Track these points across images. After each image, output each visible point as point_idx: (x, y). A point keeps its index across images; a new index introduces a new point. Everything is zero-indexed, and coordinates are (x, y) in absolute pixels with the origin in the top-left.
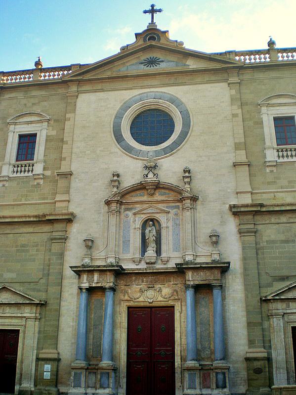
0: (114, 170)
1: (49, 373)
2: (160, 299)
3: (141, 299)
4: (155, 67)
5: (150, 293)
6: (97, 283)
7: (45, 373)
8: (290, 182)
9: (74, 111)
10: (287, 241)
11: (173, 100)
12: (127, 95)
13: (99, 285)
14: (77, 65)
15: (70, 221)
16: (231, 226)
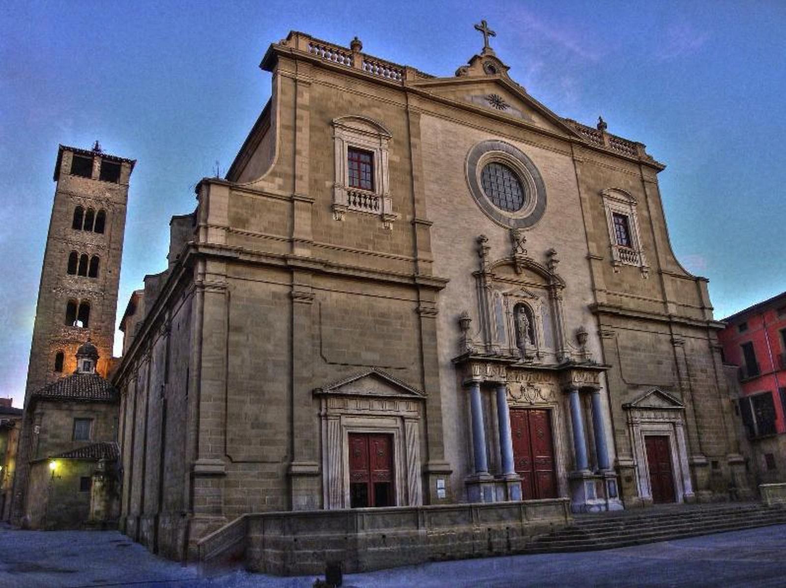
0: (484, 234)
1: (443, 491)
2: (540, 400)
3: (523, 399)
4: (501, 111)
5: (532, 393)
6: (491, 376)
7: (439, 491)
8: (631, 287)
9: (418, 135)
10: (635, 349)
11: (525, 159)
12: (486, 137)
13: (493, 379)
14: (414, 69)
15: (437, 289)
16: (591, 327)
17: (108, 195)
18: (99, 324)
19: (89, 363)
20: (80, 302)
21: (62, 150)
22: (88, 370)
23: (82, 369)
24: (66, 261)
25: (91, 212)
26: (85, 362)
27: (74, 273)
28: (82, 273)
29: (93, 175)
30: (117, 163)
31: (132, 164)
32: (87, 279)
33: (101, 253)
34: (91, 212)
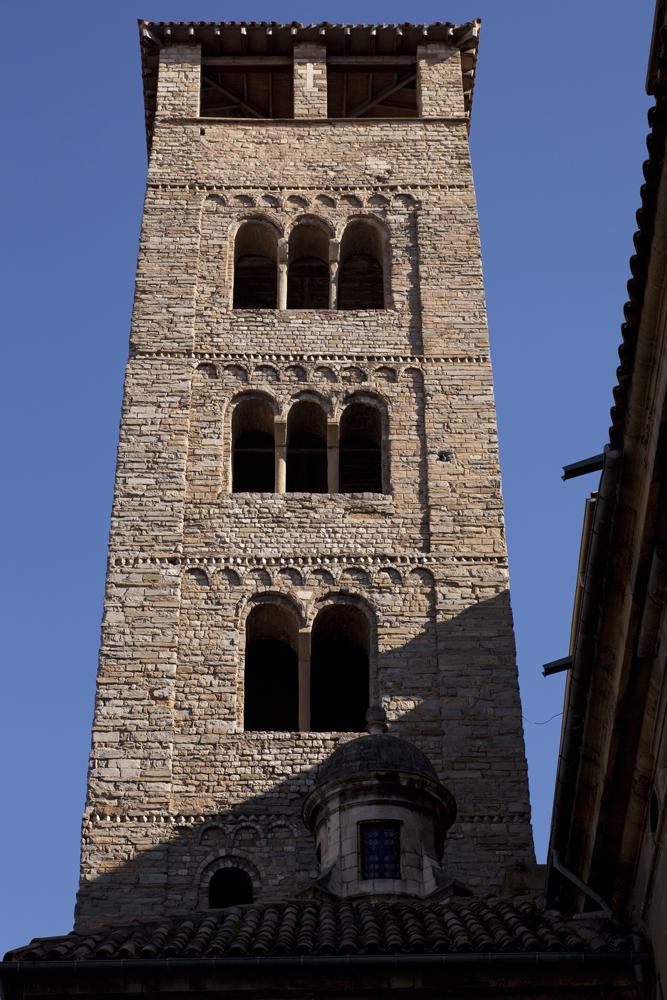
17: (378, 165)
18: (433, 704)
19: (396, 825)
20: (311, 612)
21: (158, 43)
22: (396, 874)
23: (351, 870)
24: (220, 443)
25: (311, 232)
26: (364, 827)
27: (269, 486)
28: (307, 479)
29: (299, 109)
30: (403, 61)
31: (460, 41)
32: (331, 506)
33: (375, 383)
34: (311, 232)
